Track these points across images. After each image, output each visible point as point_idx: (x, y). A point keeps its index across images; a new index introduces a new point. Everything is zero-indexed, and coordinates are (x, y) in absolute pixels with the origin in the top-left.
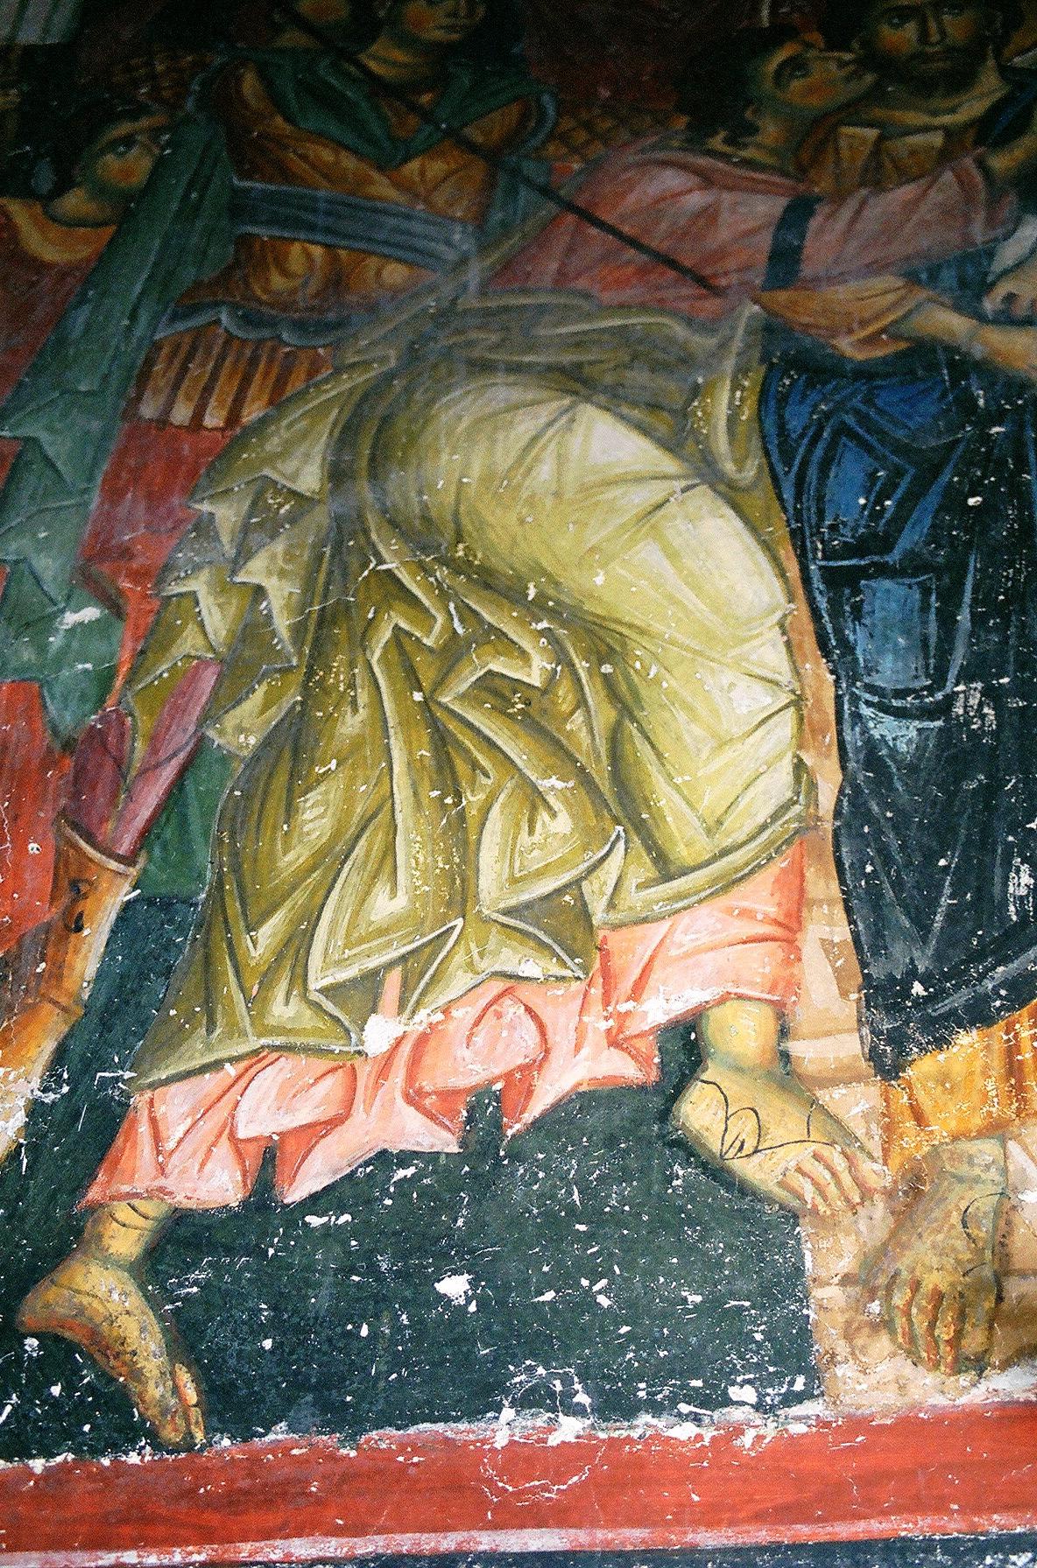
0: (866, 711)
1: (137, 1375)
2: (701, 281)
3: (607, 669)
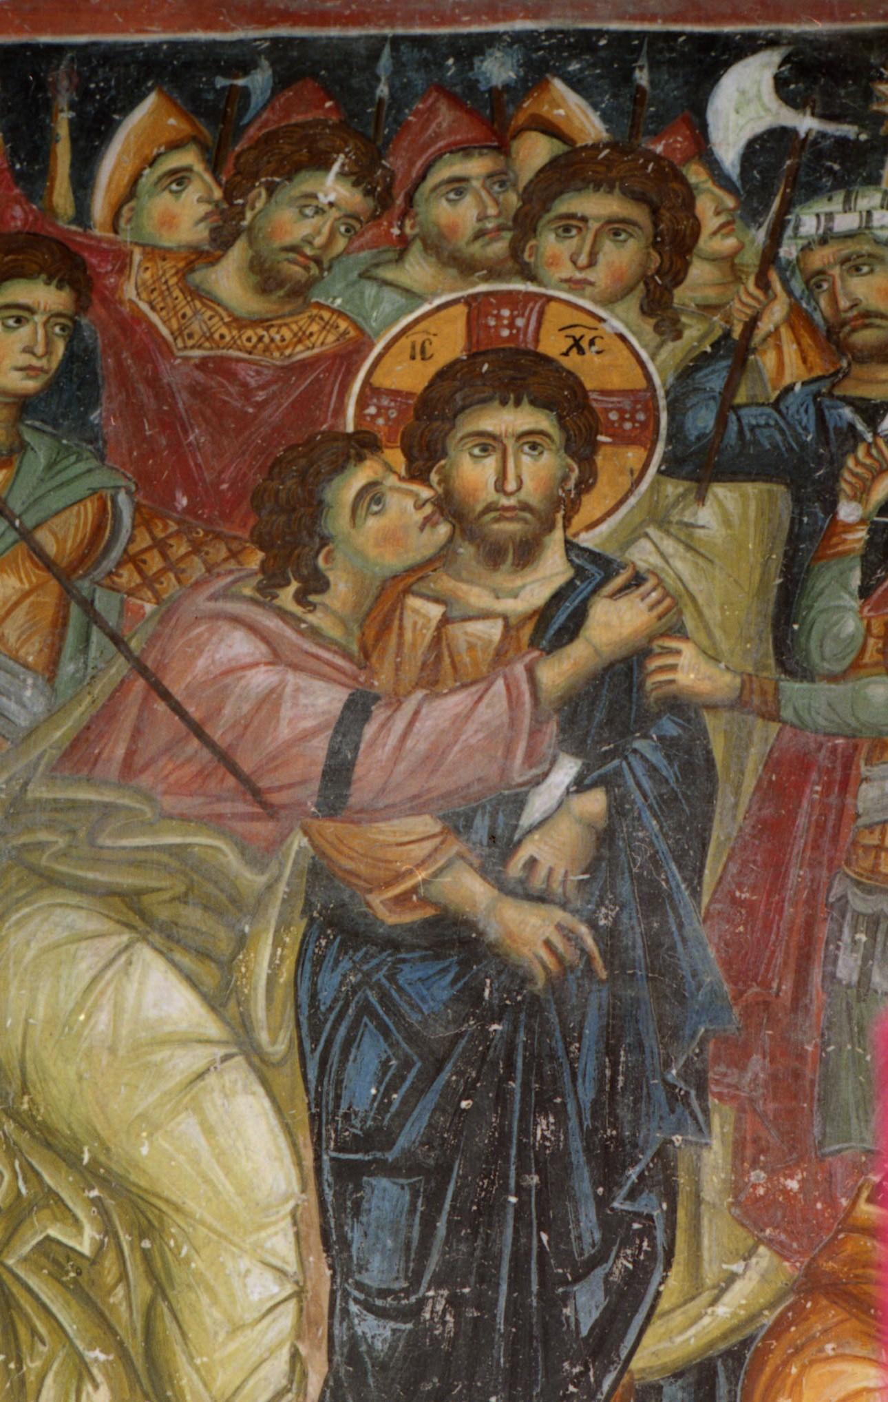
0: (354, 1308)
2: (256, 794)
3: (146, 1244)
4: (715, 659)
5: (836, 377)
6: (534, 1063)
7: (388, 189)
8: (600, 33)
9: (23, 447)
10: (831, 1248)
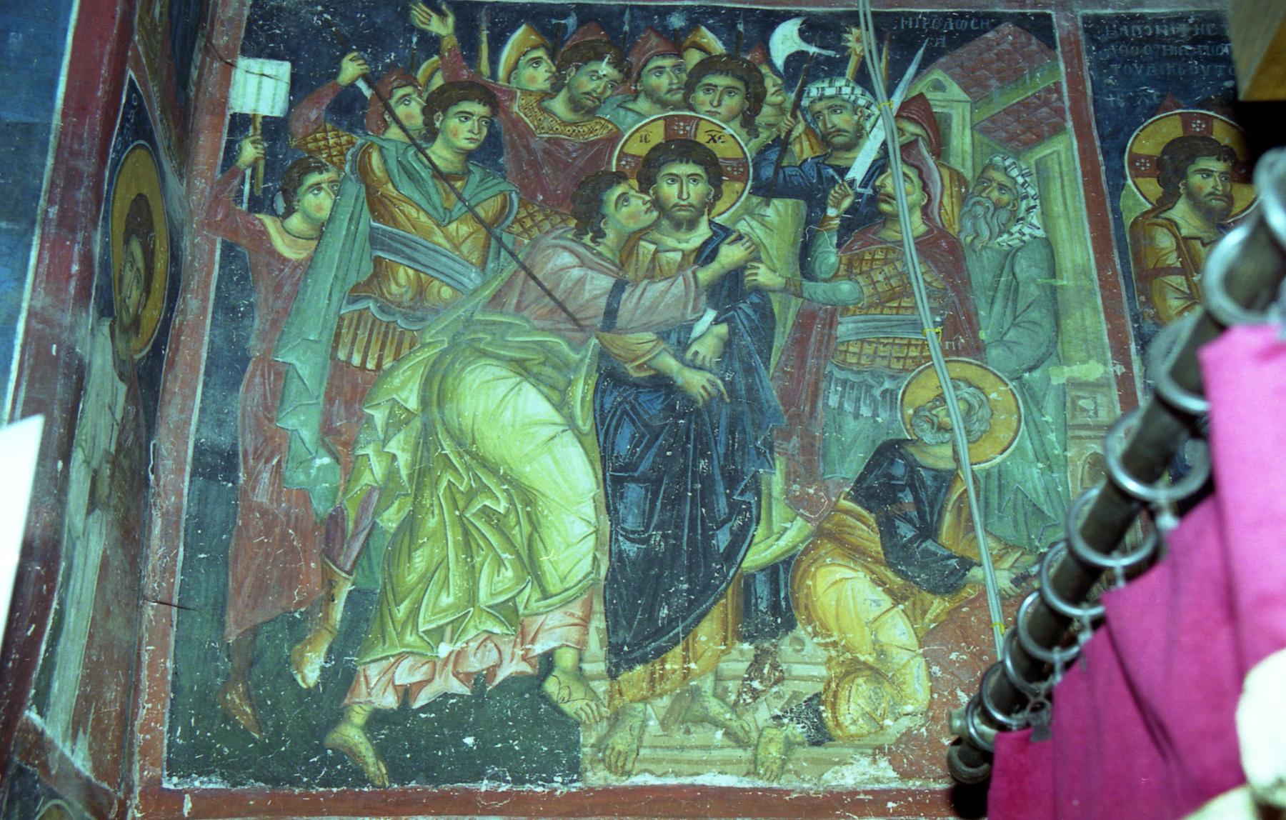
0: (621, 538)
1: (366, 763)
2: (575, 321)
4: (774, 271)
5: (826, 156)
6: (699, 437)
7: (630, 69)
8: (722, 8)
9: (470, 172)
10: (828, 518)
